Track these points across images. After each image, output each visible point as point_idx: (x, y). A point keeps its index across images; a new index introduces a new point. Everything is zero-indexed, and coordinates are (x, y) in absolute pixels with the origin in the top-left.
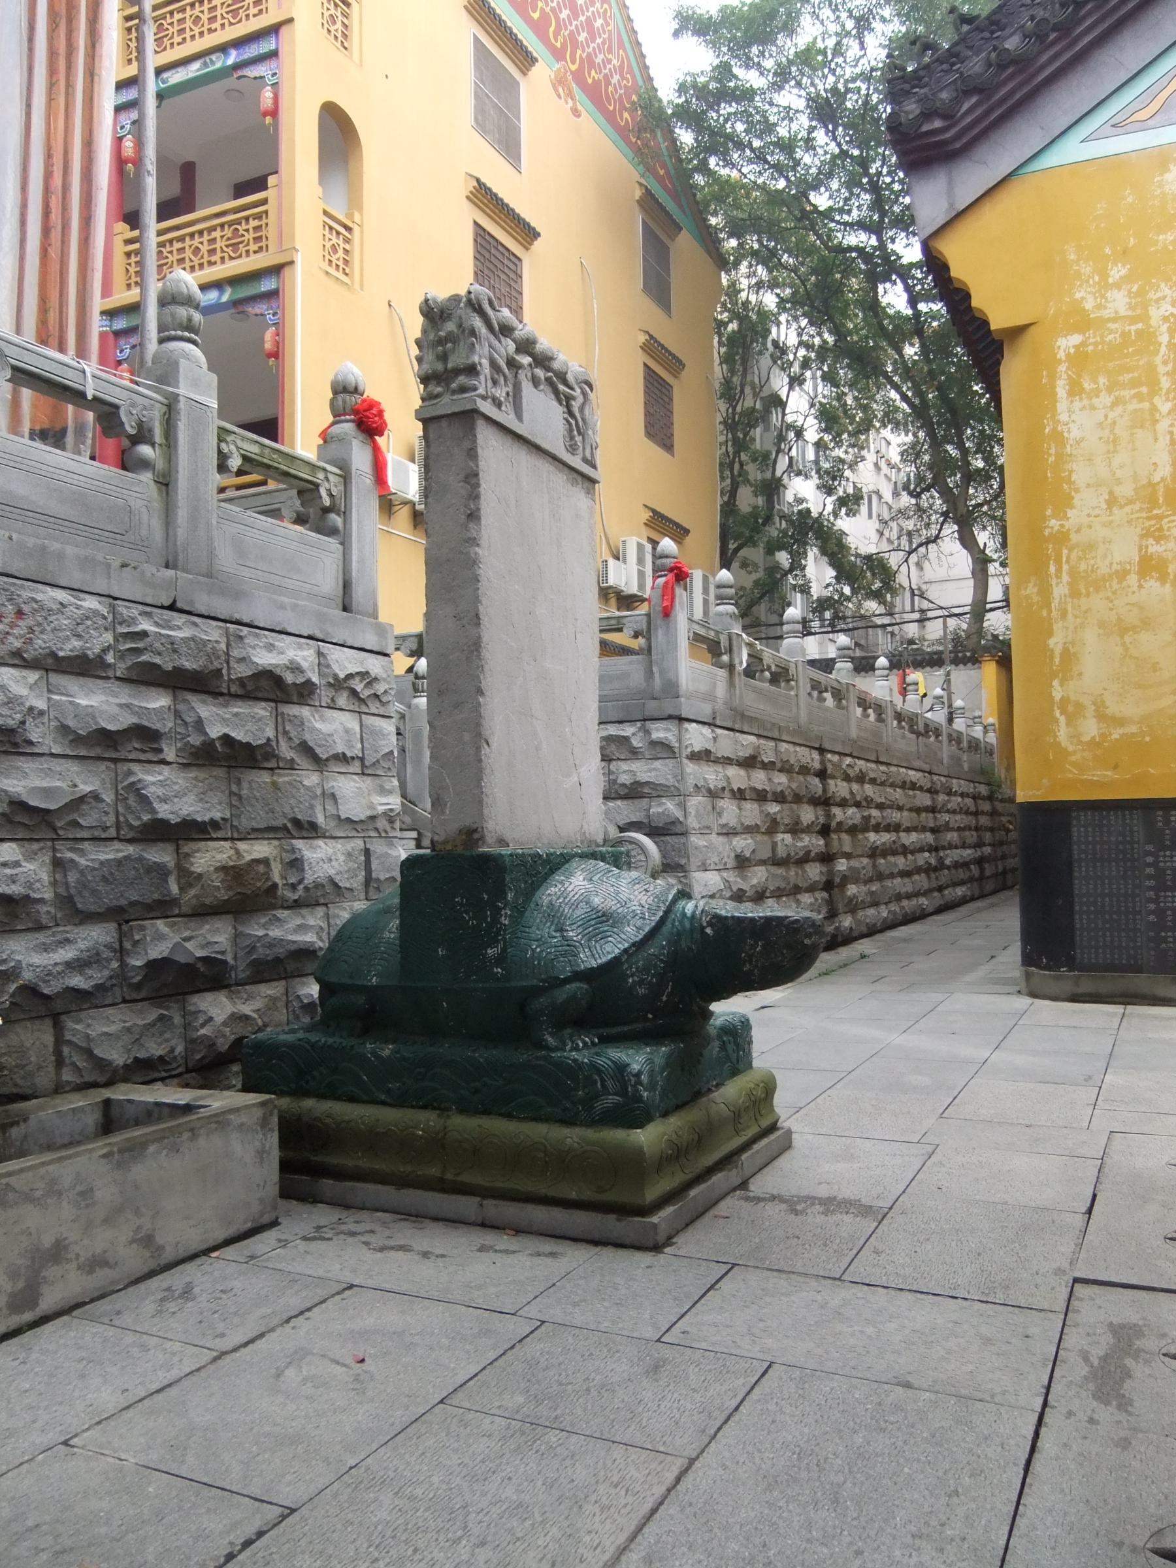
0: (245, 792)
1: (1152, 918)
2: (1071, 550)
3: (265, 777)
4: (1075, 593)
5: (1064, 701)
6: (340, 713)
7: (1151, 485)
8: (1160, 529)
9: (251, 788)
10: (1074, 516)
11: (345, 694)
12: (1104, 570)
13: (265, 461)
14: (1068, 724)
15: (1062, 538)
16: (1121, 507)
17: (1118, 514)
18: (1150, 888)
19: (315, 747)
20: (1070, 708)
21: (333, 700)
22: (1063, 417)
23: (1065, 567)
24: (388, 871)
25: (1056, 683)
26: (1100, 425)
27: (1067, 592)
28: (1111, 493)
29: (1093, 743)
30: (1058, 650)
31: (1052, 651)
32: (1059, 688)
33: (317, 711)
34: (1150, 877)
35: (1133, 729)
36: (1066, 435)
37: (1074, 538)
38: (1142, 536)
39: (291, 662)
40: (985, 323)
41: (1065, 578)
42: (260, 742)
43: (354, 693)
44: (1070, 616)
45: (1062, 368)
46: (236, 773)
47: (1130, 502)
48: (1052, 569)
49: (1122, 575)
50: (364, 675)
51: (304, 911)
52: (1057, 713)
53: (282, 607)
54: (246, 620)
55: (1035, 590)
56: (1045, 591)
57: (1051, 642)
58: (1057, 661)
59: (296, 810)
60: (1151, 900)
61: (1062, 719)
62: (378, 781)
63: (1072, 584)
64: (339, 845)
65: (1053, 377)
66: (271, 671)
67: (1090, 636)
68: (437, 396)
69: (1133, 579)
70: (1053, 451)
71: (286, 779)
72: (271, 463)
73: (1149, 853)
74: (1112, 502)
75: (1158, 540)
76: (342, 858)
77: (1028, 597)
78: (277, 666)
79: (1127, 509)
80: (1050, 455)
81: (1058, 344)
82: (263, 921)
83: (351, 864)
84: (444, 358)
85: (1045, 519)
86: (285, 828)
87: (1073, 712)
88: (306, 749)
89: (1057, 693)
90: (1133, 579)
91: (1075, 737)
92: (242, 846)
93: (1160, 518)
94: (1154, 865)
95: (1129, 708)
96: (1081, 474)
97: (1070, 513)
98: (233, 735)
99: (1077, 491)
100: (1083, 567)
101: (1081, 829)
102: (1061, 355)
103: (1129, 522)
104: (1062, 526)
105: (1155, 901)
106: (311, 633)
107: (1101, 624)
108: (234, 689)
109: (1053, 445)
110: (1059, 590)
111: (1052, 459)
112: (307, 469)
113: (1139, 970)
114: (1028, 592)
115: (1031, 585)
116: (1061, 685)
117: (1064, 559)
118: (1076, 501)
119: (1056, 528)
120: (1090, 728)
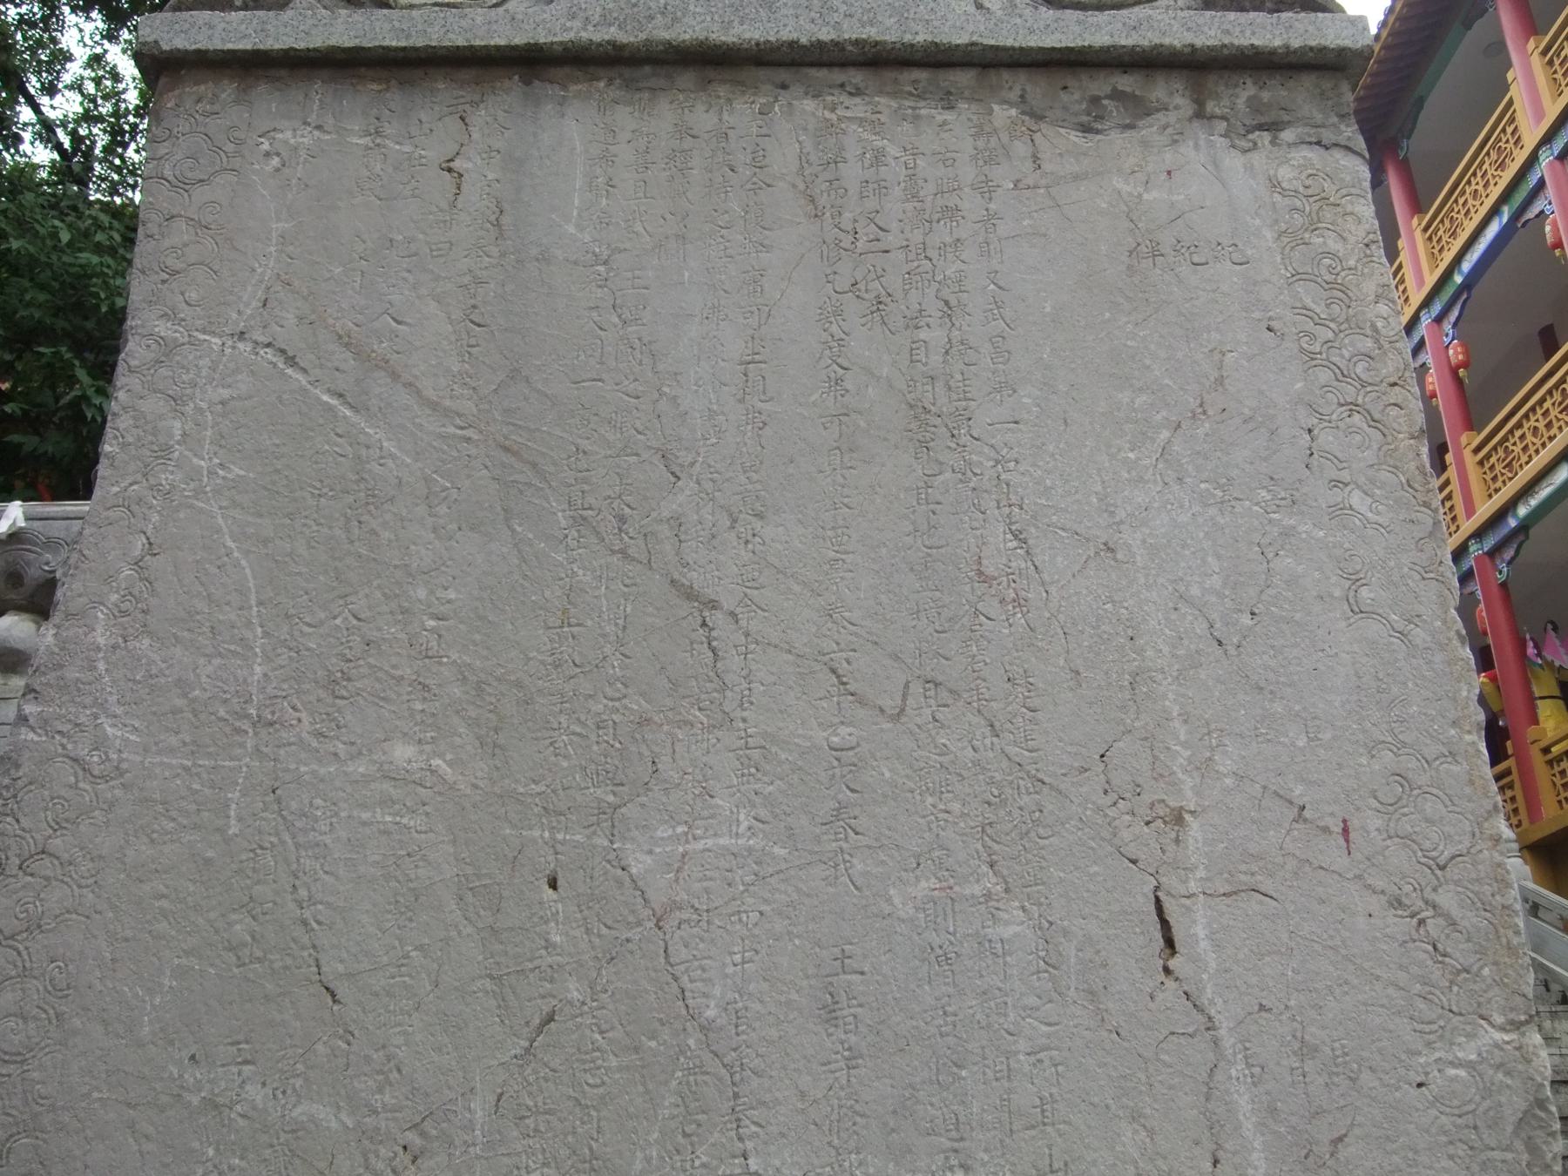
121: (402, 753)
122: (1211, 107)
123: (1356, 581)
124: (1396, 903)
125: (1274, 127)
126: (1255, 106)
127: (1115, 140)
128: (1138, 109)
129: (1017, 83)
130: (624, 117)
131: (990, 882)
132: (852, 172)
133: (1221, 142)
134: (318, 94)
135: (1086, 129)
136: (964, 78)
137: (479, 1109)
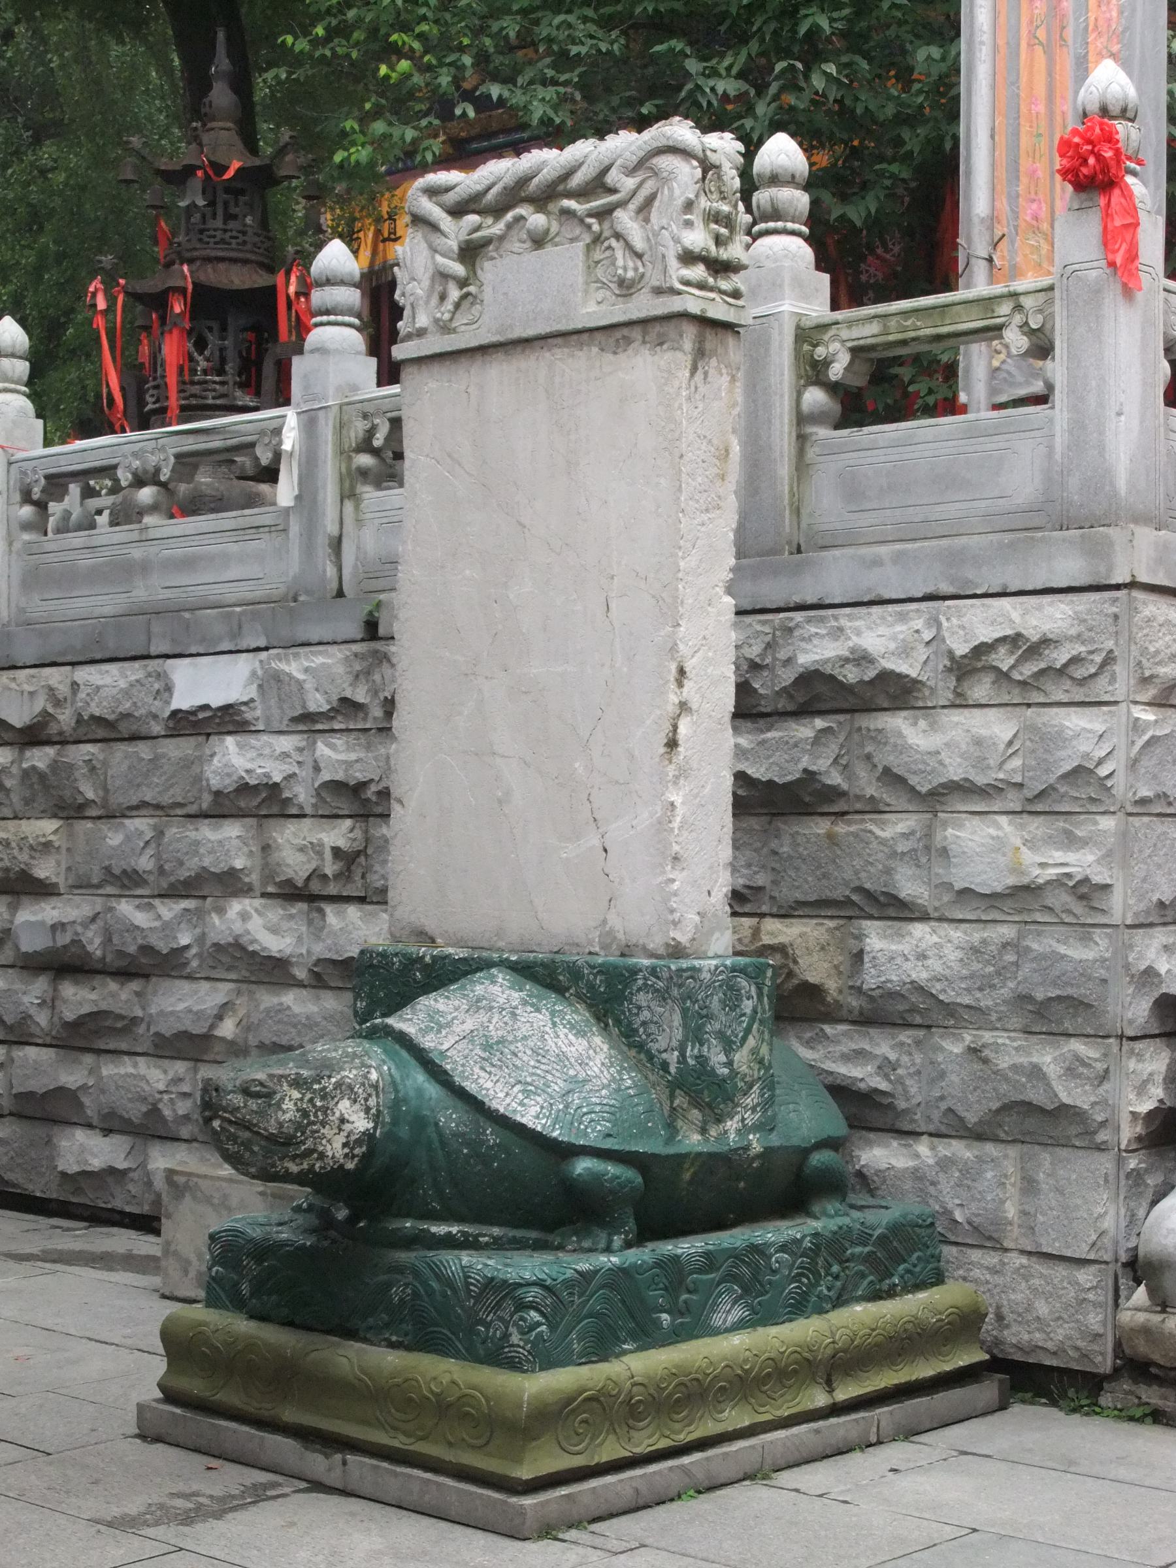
0: (785, 849)
3: (821, 826)
6: (976, 711)
9: (795, 845)
11: (987, 679)
13: (891, 338)
19: (906, 775)
21: (959, 695)
24: (1054, 984)
33: (926, 717)
39: (853, 650)
42: (789, 778)
43: (1003, 677)
46: (779, 823)
50: (1014, 640)
51: (873, 1031)
53: (877, 562)
54: (811, 599)
59: (863, 875)
62: (1061, 824)
64: (956, 934)
66: (817, 671)
71: (853, 829)
72: (900, 336)
76: (952, 955)
78: (827, 661)
82: (808, 1035)
83: (976, 966)
86: (848, 902)
88: (892, 778)
92: (770, 925)
98: (749, 772)
106: (930, 589)
108: (784, 704)
112: (975, 311)
121: (467, 572)
122: (647, 338)
123: (659, 507)
124: (653, 597)
125: (661, 344)
126: (659, 335)
127: (622, 357)
128: (628, 341)
129: (598, 336)
130: (505, 366)
131: (575, 596)
132: (557, 380)
133: (647, 352)
134: (436, 368)
135: (615, 353)
136: (585, 336)
137: (485, 654)
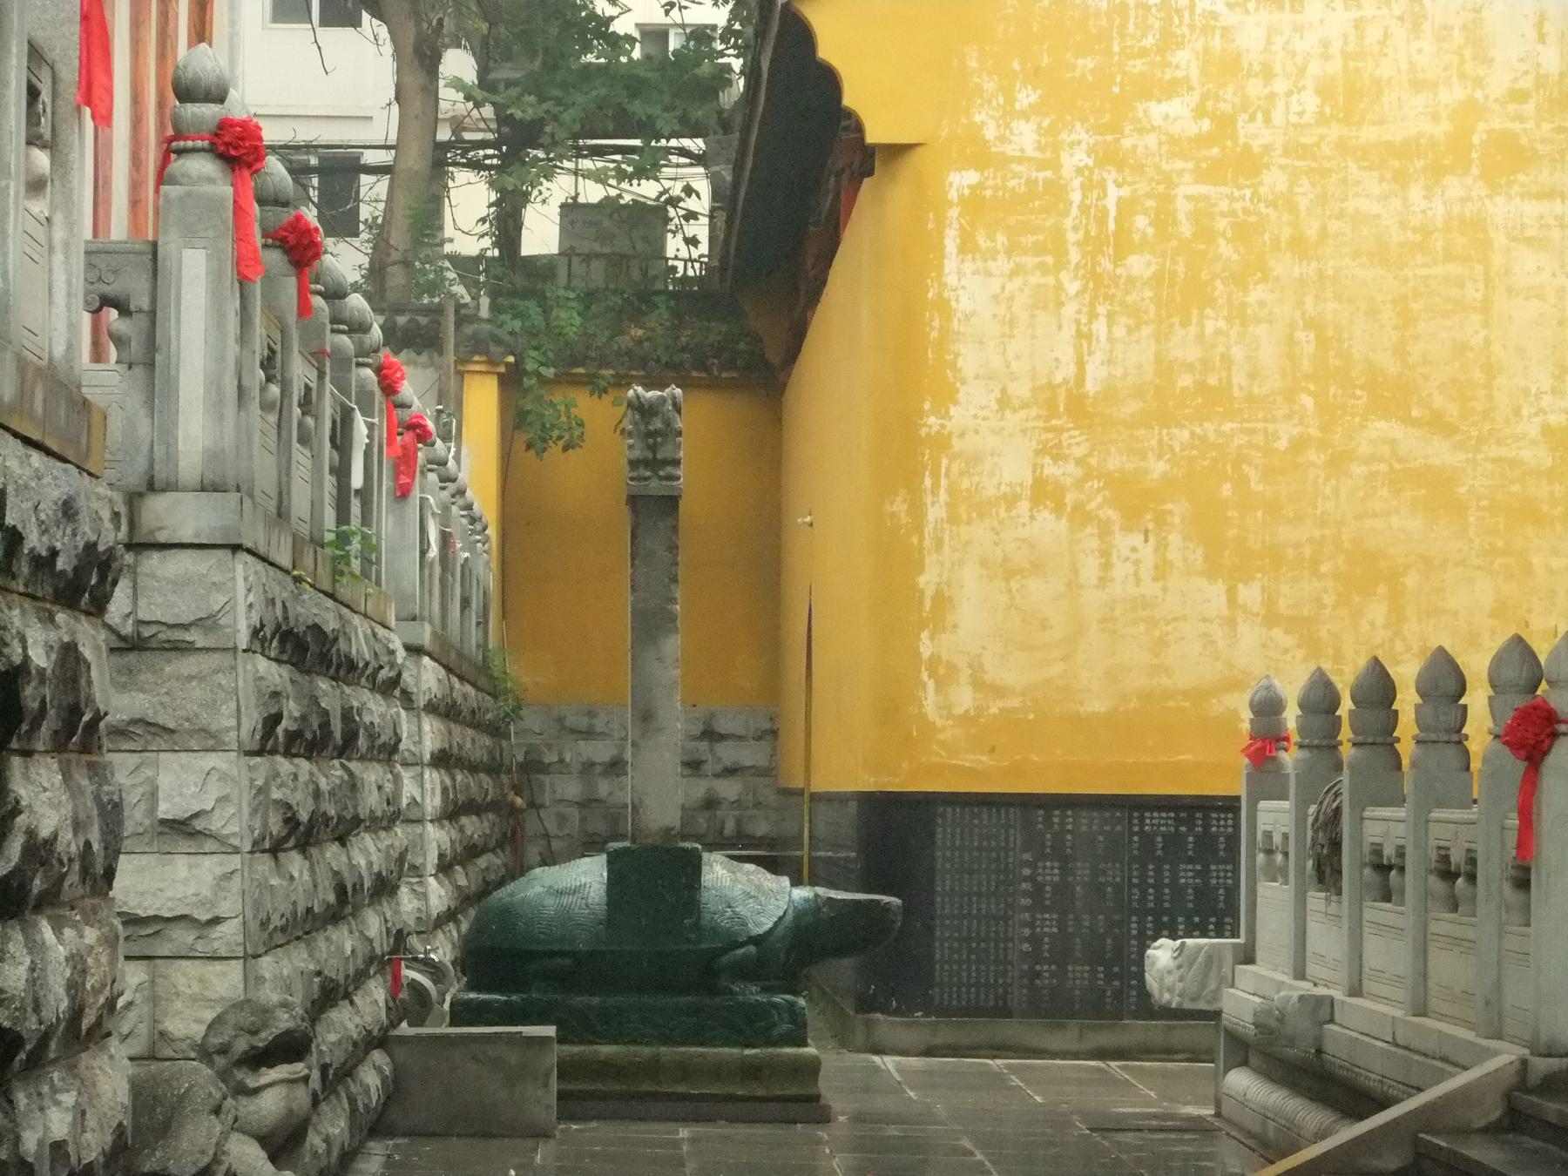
1: (1026, 947)
2: (952, 459)
4: (953, 519)
5: (934, 662)
7: (1051, 386)
8: (1059, 445)
10: (959, 416)
12: (990, 492)
14: (937, 691)
15: (941, 442)
16: (1015, 410)
17: (1012, 420)
18: (1026, 909)
20: (942, 671)
22: (951, 280)
23: (944, 482)
25: (924, 635)
26: (995, 298)
27: (944, 516)
28: (1004, 391)
29: (967, 719)
30: (929, 592)
31: (922, 592)
32: (928, 642)
34: (1026, 894)
35: (1014, 702)
36: (953, 304)
37: (957, 444)
38: (1038, 452)
40: (859, 128)
41: (943, 496)
44: (946, 548)
45: (953, 213)
47: (1026, 405)
48: (928, 482)
49: (1011, 500)
52: (925, 676)
55: (905, 507)
56: (917, 510)
57: (922, 580)
58: (928, 605)
60: (1024, 924)
61: (931, 684)
63: (951, 506)
65: (941, 225)
67: (970, 582)
68: (646, 479)
69: (1024, 507)
70: (936, 324)
73: (1027, 864)
74: (1004, 402)
75: (1057, 458)
77: (893, 515)
79: (1022, 414)
80: (932, 329)
81: (951, 178)
84: (653, 448)
85: (921, 414)
87: (945, 675)
89: (926, 650)
90: (1024, 507)
91: (945, 709)
93: (1059, 430)
94: (1031, 879)
95: (1010, 674)
96: (969, 360)
97: (953, 411)
99: (963, 382)
100: (965, 484)
101: (945, 831)
102: (953, 195)
103: (1024, 431)
104: (943, 426)
105: (1032, 925)
107: (984, 563)
109: (936, 316)
110: (935, 512)
111: (935, 334)
113: (1002, 1011)
114: (895, 508)
115: (899, 499)
116: (932, 639)
117: (943, 471)
118: (961, 396)
119: (935, 429)
120: (964, 698)
